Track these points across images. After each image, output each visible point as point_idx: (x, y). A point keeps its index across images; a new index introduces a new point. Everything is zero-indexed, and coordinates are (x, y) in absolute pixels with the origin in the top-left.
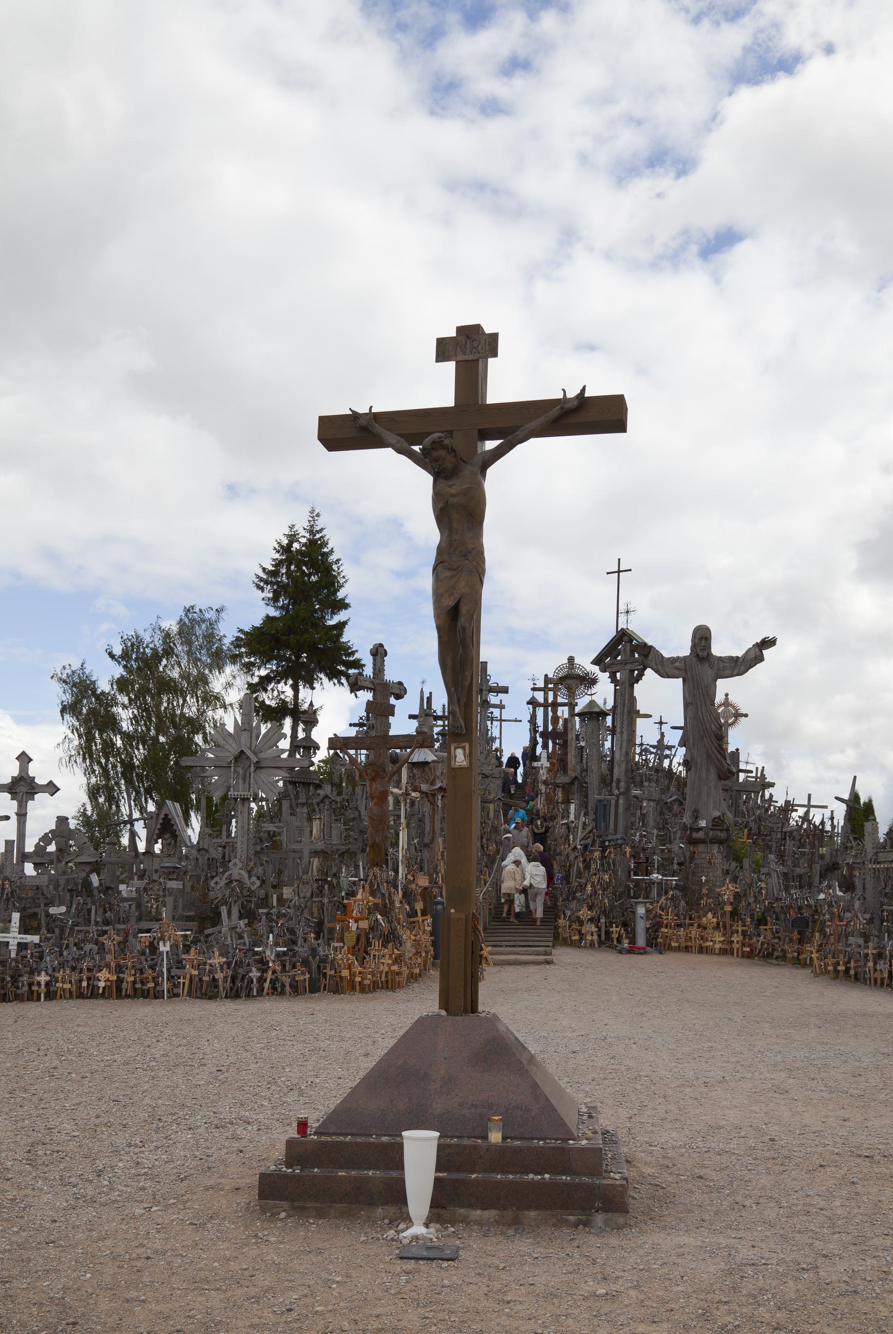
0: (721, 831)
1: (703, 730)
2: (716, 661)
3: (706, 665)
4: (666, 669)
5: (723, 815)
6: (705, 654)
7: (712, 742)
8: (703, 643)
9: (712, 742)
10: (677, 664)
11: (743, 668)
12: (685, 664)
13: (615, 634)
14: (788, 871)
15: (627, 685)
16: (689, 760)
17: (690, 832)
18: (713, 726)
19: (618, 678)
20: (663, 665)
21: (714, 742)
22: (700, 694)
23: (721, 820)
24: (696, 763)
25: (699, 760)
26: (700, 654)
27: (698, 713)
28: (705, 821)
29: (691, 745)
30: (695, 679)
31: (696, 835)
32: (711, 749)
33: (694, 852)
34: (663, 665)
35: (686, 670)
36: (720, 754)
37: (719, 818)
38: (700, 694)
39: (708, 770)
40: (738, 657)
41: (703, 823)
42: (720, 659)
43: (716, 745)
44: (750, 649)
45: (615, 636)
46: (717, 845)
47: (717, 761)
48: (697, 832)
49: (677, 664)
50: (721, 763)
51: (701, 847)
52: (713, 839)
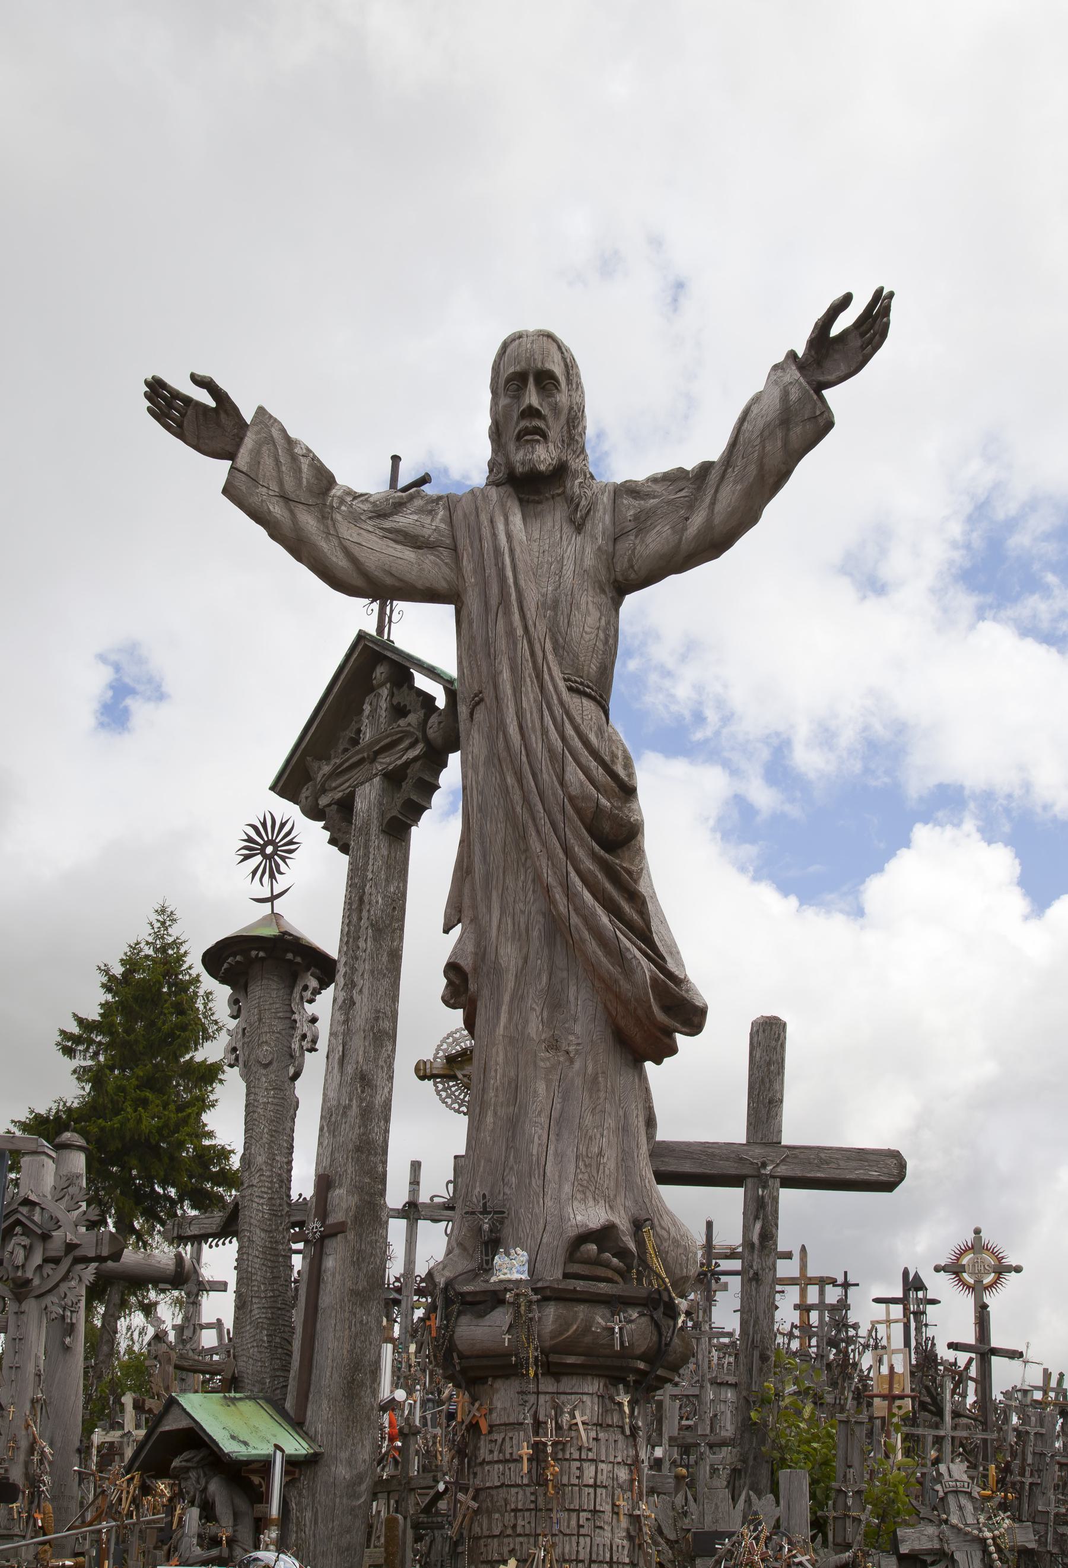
0: (615, 1303)
1: (526, 799)
2: (605, 499)
3: (555, 518)
4: (349, 532)
5: (637, 1225)
6: (544, 456)
7: (567, 850)
8: (532, 398)
9: (567, 850)
10: (405, 520)
12: (450, 521)
14: (1042, 1541)
15: (374, 829)
16: (466, 963)
18: (574, 775)
20: (325, 514)
21: (579, 852)
22: (510, 633)
23: (622, 1253)
24: (498, 971)
25: (509, 955)
27: (502, 726)
28: (522, 1256)
29: (479, 895)
30: (491, 571)
32: (567, 888)
33: (474, 1427)
34: (325, 514)
35: (455, 549)
37: (605, 1235)
38: (510, 633)
39: (555, 1003)
40: (706, 468)
42: (630, 489)
43: (589, 864)
44: (756, 399)
46: (594, 1386)
47: (592, 946)
48: (481, 1315)
49: (405, 520)
50: (619, 956)
52: (567, 1348)
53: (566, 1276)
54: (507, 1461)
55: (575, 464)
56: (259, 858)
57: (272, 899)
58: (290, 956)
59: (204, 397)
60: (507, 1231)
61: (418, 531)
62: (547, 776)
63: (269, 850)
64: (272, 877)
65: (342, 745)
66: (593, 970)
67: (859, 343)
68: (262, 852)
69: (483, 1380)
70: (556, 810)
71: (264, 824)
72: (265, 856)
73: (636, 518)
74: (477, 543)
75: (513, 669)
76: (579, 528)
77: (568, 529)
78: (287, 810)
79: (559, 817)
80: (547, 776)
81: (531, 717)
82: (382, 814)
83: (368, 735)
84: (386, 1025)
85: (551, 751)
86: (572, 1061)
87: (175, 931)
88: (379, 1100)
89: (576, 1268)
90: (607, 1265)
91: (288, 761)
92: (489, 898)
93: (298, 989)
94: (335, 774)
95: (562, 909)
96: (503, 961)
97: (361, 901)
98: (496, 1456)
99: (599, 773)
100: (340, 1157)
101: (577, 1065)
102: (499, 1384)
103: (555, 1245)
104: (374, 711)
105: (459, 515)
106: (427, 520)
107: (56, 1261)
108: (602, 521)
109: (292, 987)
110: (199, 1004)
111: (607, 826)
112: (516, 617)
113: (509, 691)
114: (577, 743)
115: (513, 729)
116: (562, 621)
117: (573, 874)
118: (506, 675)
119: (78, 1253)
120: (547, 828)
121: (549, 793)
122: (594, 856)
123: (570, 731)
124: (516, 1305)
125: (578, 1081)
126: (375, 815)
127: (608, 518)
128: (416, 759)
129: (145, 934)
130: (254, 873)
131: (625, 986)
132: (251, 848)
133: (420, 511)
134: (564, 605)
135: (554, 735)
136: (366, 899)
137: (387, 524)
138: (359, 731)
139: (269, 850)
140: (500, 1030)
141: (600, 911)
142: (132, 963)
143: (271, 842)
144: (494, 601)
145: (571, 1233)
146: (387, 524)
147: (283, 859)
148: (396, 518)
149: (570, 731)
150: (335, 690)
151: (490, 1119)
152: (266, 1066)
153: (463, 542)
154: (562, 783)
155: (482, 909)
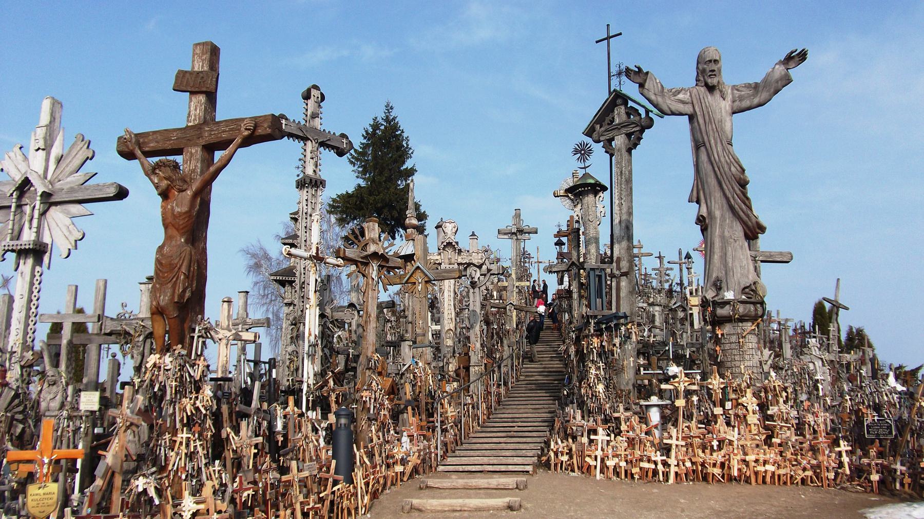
10: (681, 96)
11: (764, 96)
12: (691, 96)
13: (607, 96)
15: (624, 151)
17: (714, 308)
18: (733, 169)
19: (614, 147)
22: (713, 130)
26: (709, 81)
31: (720, 312)
35: (693, 103)
36: (745, 204)
38: (713, 130)
40: (756, 83)
41: (729, 295)
43: (739, 192)
45: (607, 99)
48: (722, 308)
49: (681, 96)
50: (748, 216)
51: (727, 329)
54: (731, 343)
55: (721, 82)
56: (579, 154)
57: (585, 168)
58: (597, 188)
59: (637, 70)
61: (683, 100)
62: (726, 169)
63: (583, 152)
64: (584, 161)
67: (798, 59)
68: (581, 153)
69: (723, 323)
70: (729, 178)
71: (581, 144)
72: (581, 154)
73: (738, 97)
74: (700, 104)
75: (714, 139)
76: (724, 99)
77: (721, 99)
78: (588, 140)
79: (730, 180)
80: (726, 169)
81: (721, 153)
83: (617, 121)
84: (630, 210)
85: (726, 162)
86: (736, 241)
87: (393, 114)
88: (631, 234)
90: (750, 294)
93: (597, 197)
95: (733, 203)
96: (716, 215)
97: (621, 172)
98: (727, 342)
99: (738, 168)
100: (623, 252)
101: (737, 243)
103: (738, 289)
104: (619, 114)
105: (693, 95)
106: (686, 96)
107: (485, 275)
108: (729, 97)
109: (595, 196)
110: (404, 143)
111: (742, 182)
112: (714, 126)
113: (714, 145)
114: (732, 160)
116: (723, 125)
117: (735, 195)
118: (712, 141)
119: (492, 272)
120: (728, 182)
121: (727, 173)
122: (740, 189)
123: (731, 157)
124: (734, 305)
125: (738, 247)
127: (731, 96)
128: (637, 131)
129: (380, 115)
130: (578, 159)
132: (576, 151)
133: (684, 94)
134: (723, 121)
135: (727, 158)
136: (623, 172)
137: (676, 98)
138: (613, 118)
139: (583, 152)
141: (742, 204)
142: (376, 126)
143: (584, 150)
145: (743, 286)
146: (676, 98)
147: (588, 156)
148: (679, 96)
149: (731, 157)
150: (605, 105)
152: (592, 222)
153: (695, 102)
154: (730, 170)
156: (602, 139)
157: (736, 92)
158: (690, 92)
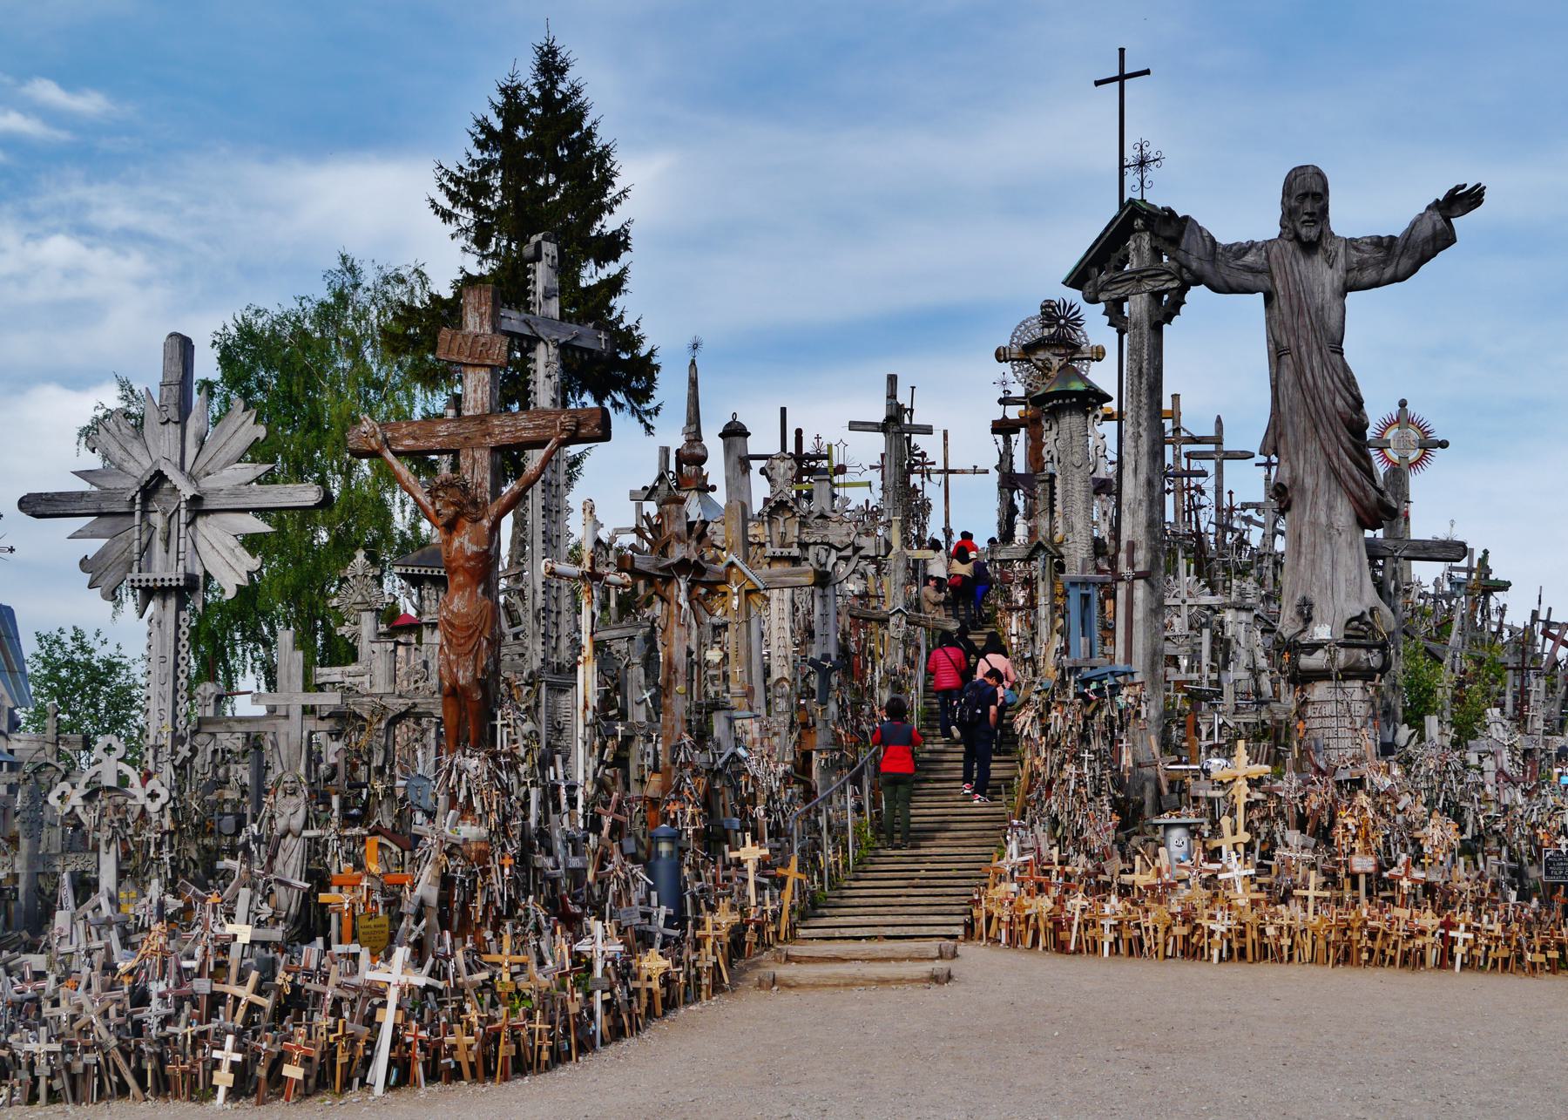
1: (1317, 411)
7: (1337, 437)
9: (1337, 437)
12: (1268, 258)
24: (1303, 491)
25: (1309, 482)
28: (1328, 628)
46: (1359, 683)
47: (1352, 485)
50: (1363, 489)
53: (1346, 636)
60: (1315, 613)
62: (1327, 402)
63: (1062, 321)
65: (1113, 262)
66: (1350, 494)
77: (1326, 266)
78: (1075, 296)
82: (1150, 317)
89: (1350, 632)
91: (1076, 268)
92: (1297, 453)
94: (1111, 282)
102: (1317, 684)
108: (1341, 262)
115: (1309, 375)
116: (1326, 316)
117: (1341, 450)
118: (1304, 349)
126: (1146, 317)
131: (1366, 502)
135: (1328, 380)
140: (1306, 519)
144: (1296, 310)
151: (1303, 561)
154: (1334, 404)
155: (1294, 458)
156: (1102, 297)
157: (1353, 252)
158: (1267, 252)
